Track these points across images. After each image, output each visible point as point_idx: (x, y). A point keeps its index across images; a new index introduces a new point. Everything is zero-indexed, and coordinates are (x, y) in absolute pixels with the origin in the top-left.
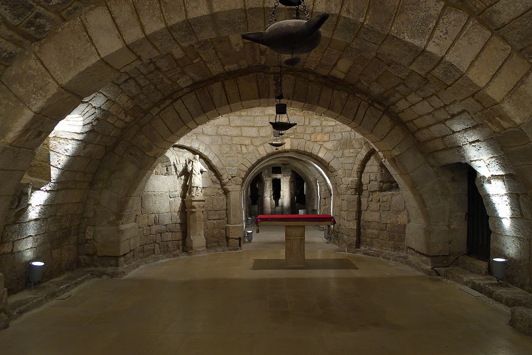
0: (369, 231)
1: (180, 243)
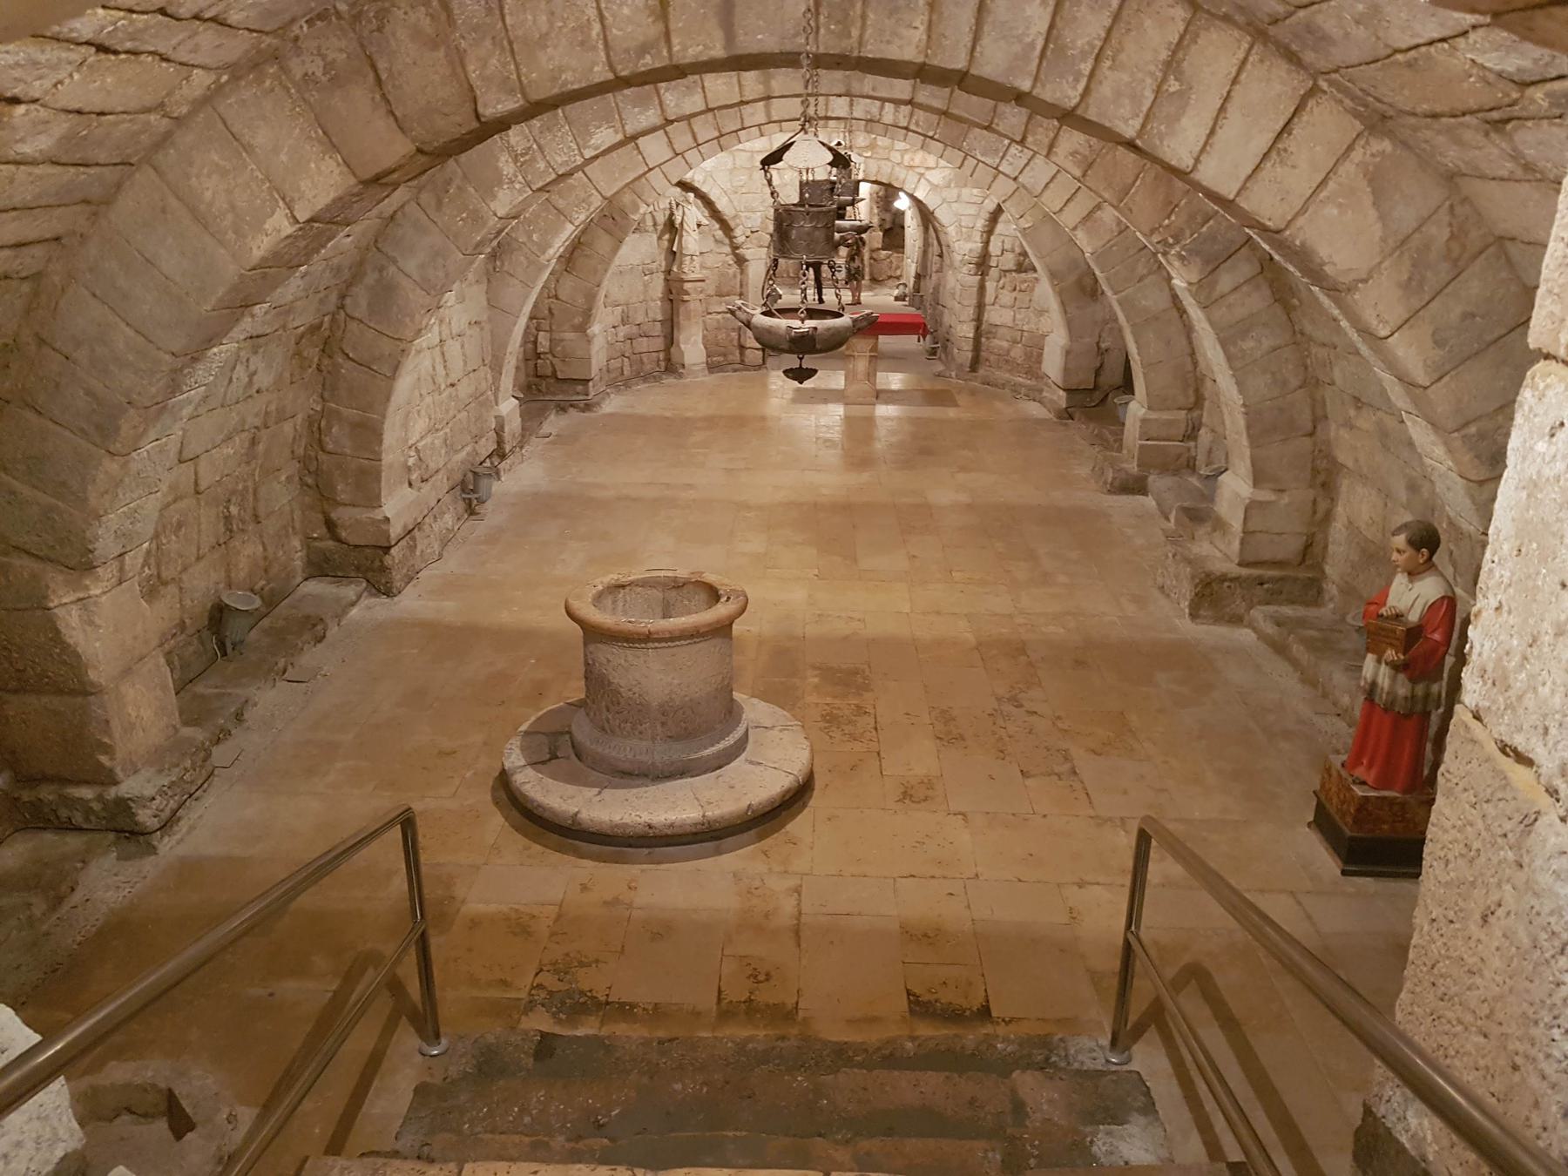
0: (996, 342)
1: (662, 356)
